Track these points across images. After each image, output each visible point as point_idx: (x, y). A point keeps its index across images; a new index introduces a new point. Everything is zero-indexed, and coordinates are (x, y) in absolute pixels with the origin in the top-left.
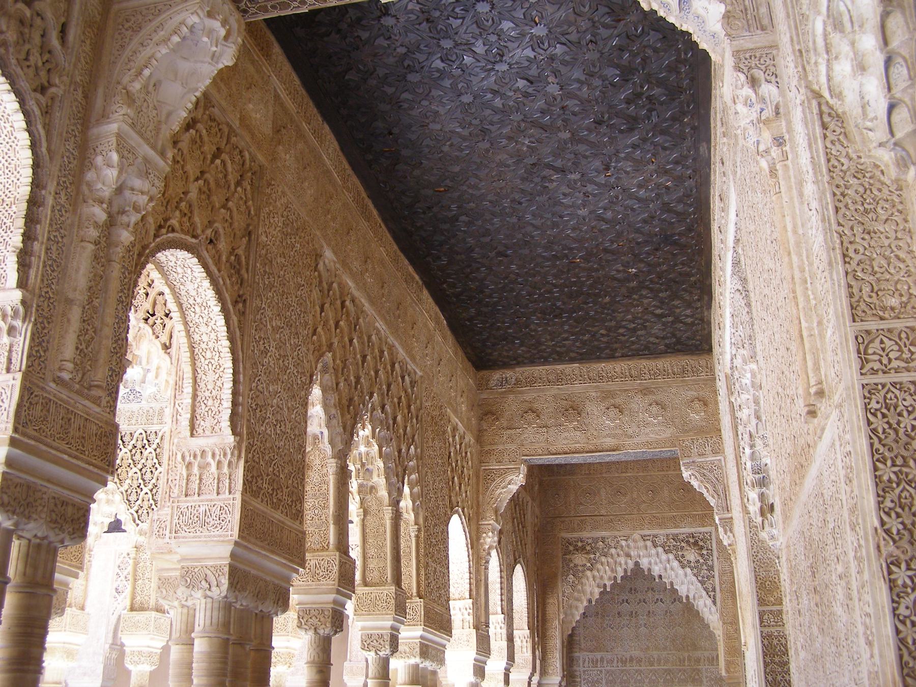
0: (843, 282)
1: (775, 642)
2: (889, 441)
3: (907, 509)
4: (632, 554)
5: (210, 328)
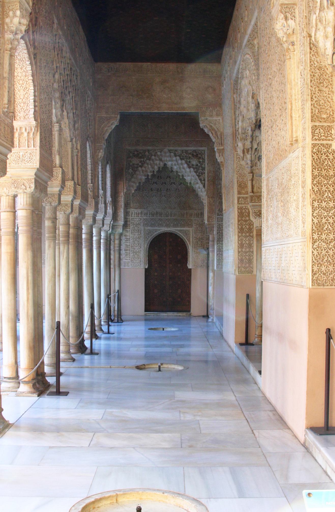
0: (310, 108)
1: (244, 211)
2: (317, 162)
3: (320, 184)
4: (163, 159)
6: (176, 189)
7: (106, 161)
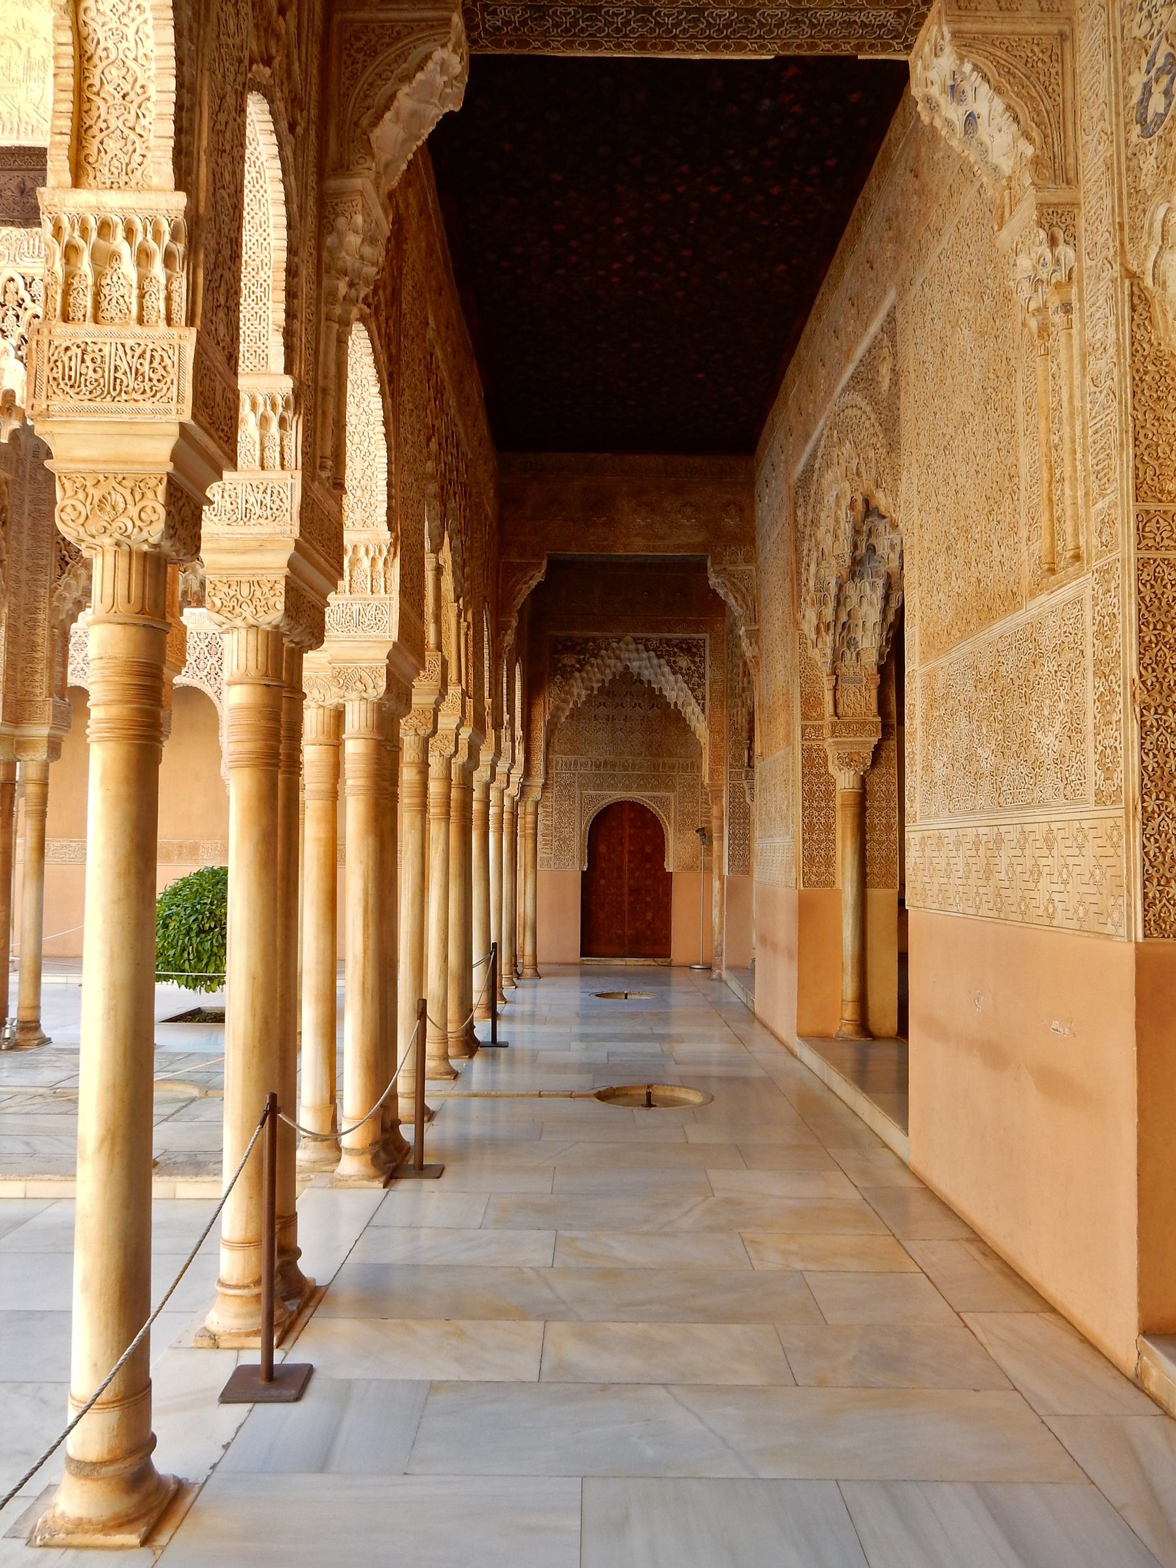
1: (814, 755)
3: (1160, 665)
4: (622, 656)
5: (361, 410)
6: (644, 717)
7: (518, 653)
